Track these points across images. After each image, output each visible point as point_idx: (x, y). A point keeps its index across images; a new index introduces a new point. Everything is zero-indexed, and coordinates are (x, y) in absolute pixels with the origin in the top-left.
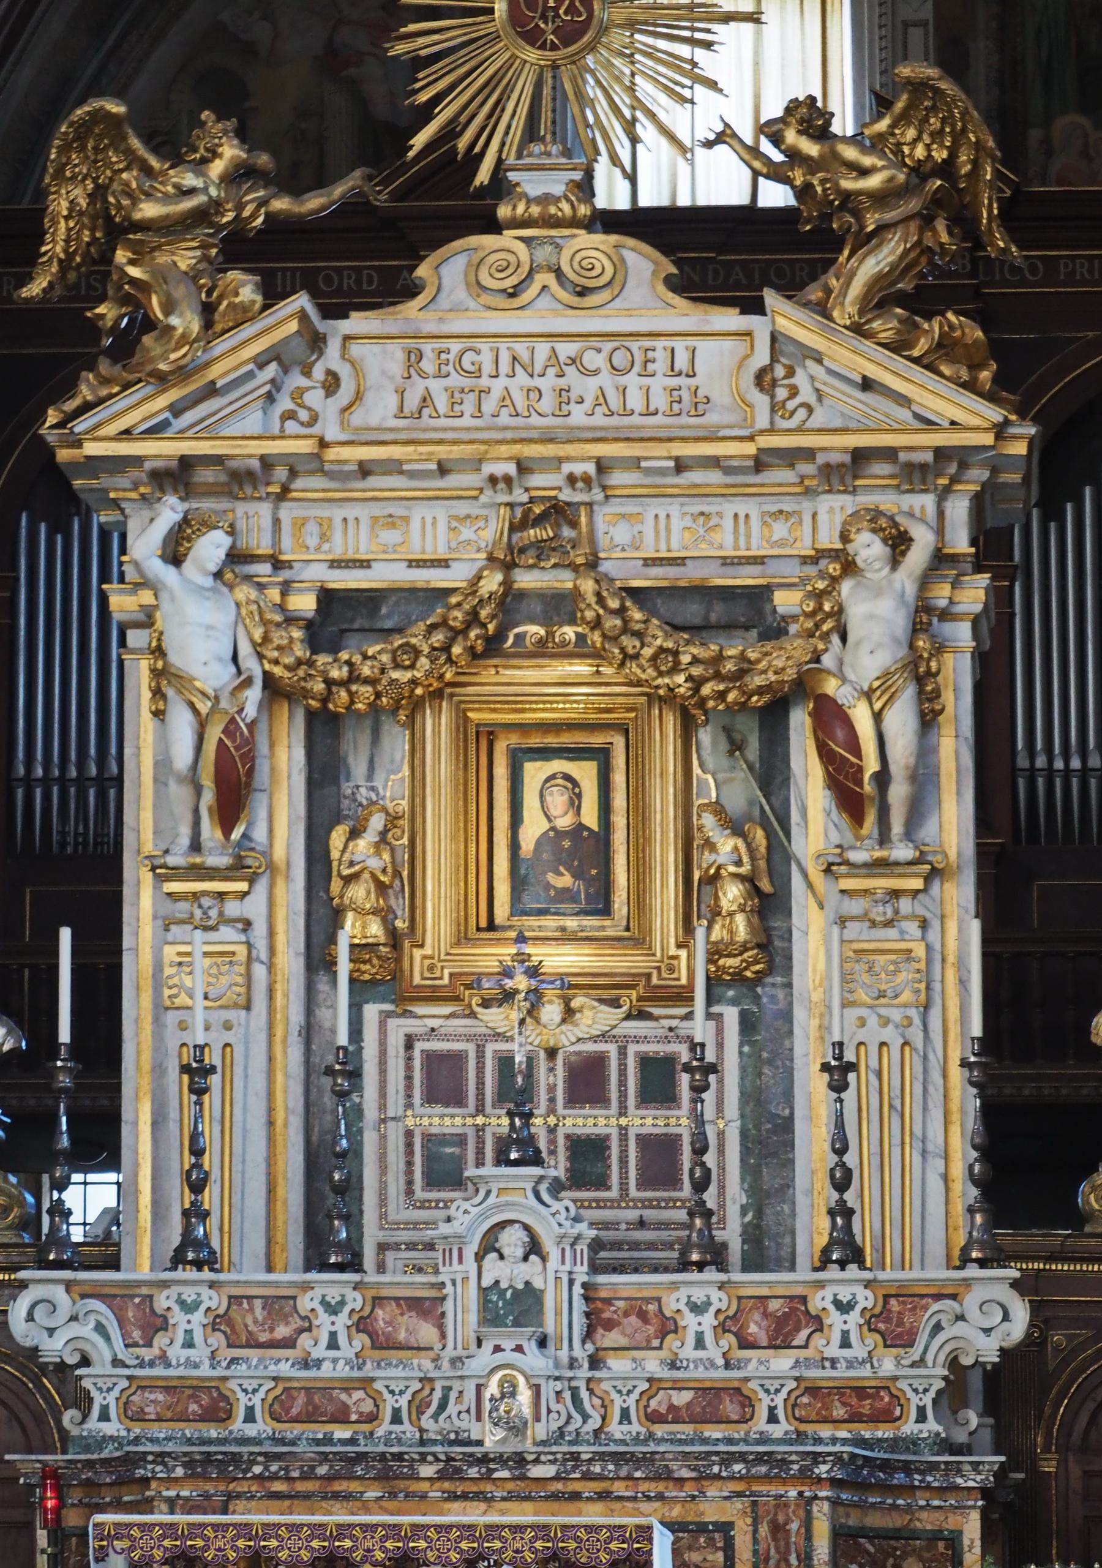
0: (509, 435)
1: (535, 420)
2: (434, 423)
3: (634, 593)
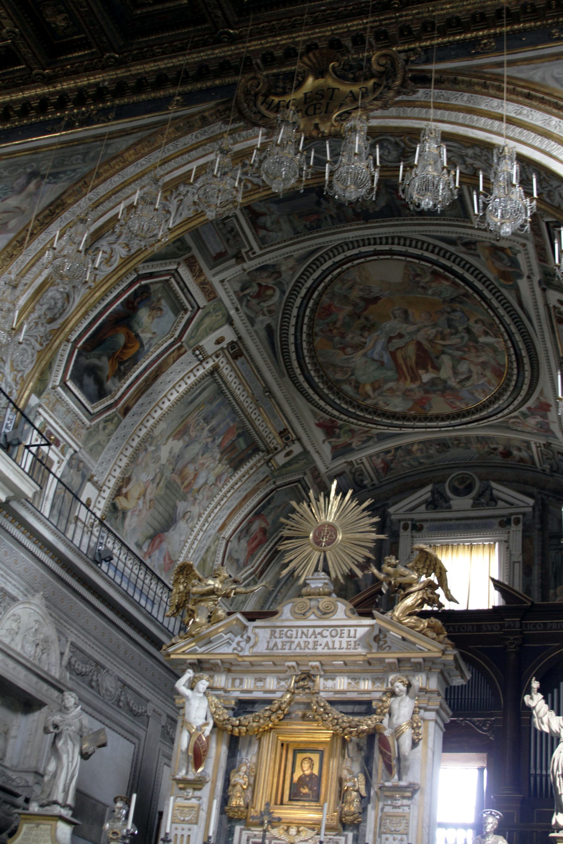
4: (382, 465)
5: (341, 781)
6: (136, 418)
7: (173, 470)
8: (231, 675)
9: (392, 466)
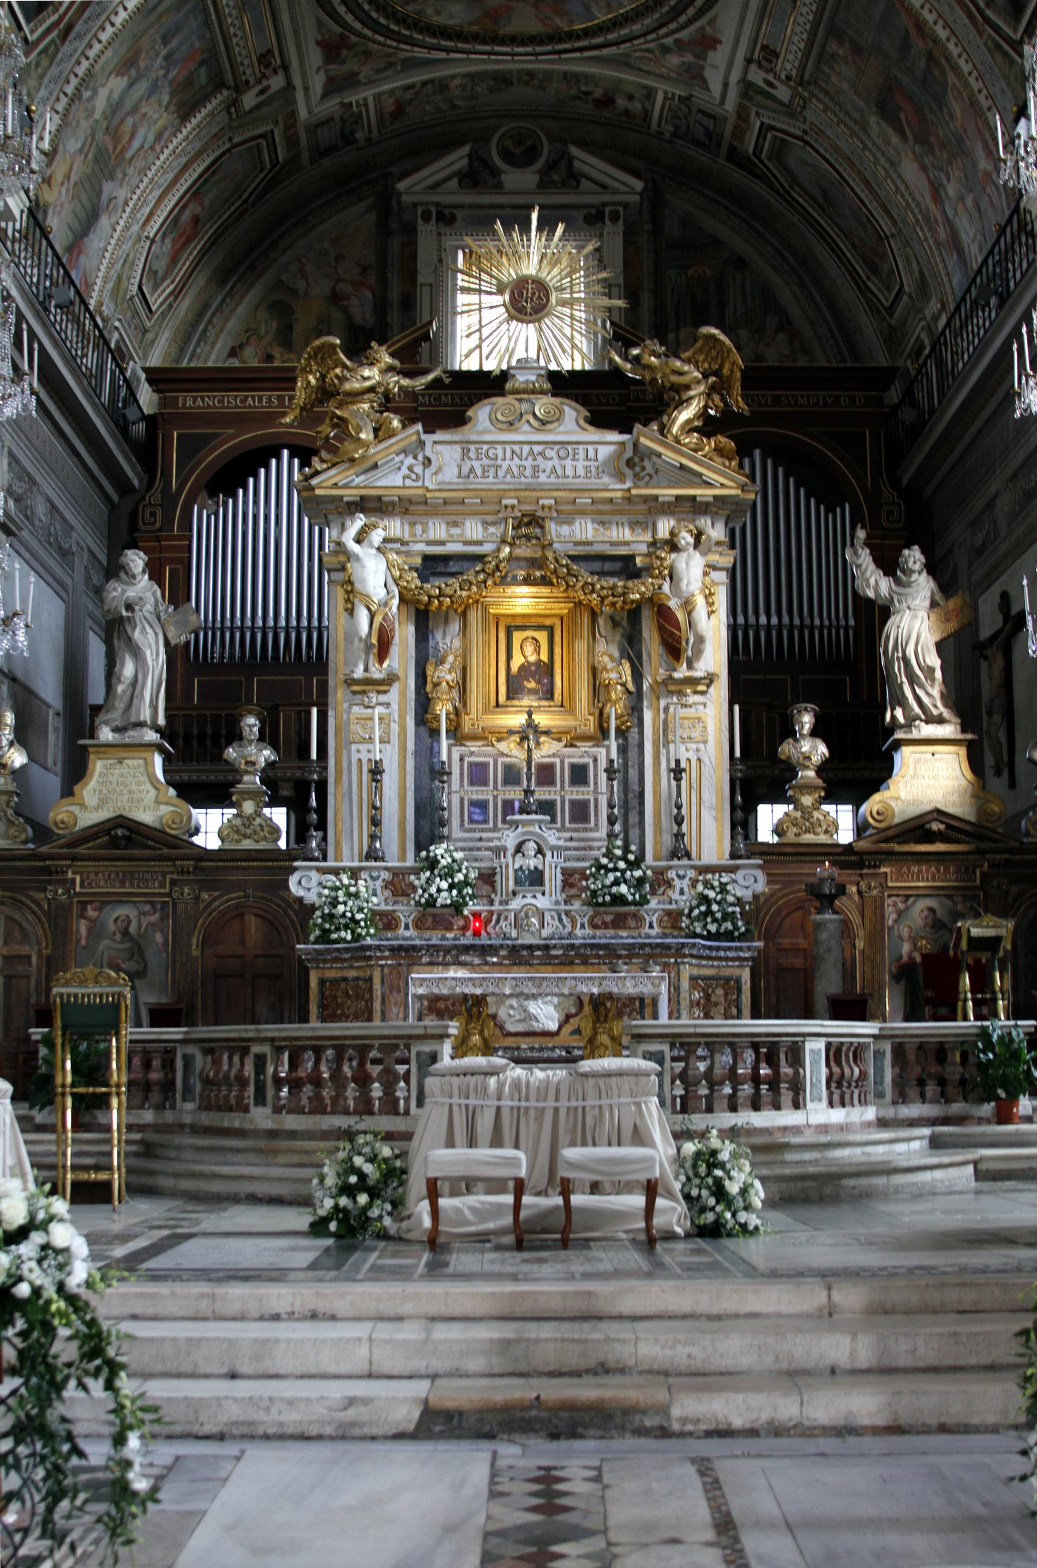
1: (523, 479)
4: (392, 108)
5: (594, 671)
6: (77, 43)
7: (107, 128)
8: (411, 518)
9: (407, 110)
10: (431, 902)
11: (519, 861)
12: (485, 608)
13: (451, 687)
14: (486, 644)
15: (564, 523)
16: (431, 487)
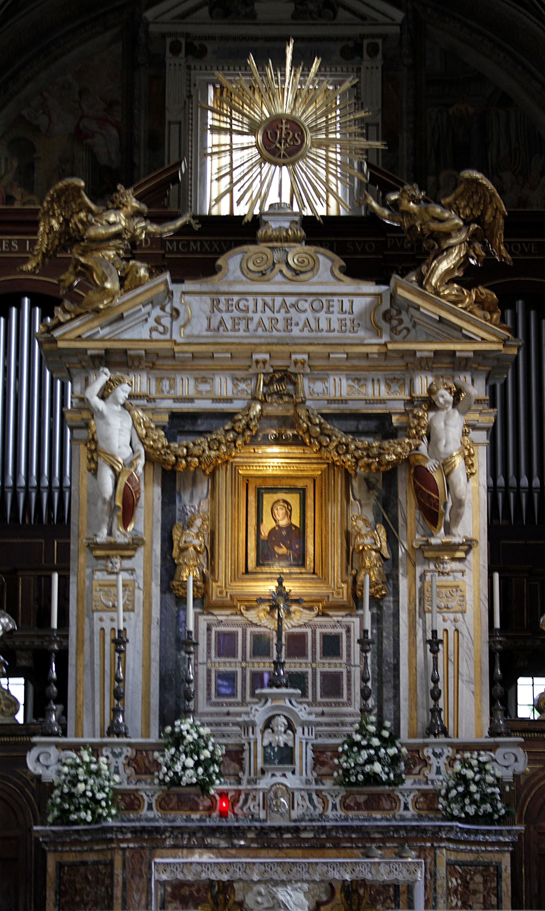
0: (263, 341)
1: (275, 333)
2: (225, 333)
3: (323, 415)
5: (348, 536)
10: (176, 780)
11: (268, 738)
12: (235, 469)
13: (198, 552)
14: (235, 507)
15: (318, 379)
16: (179, 340)
